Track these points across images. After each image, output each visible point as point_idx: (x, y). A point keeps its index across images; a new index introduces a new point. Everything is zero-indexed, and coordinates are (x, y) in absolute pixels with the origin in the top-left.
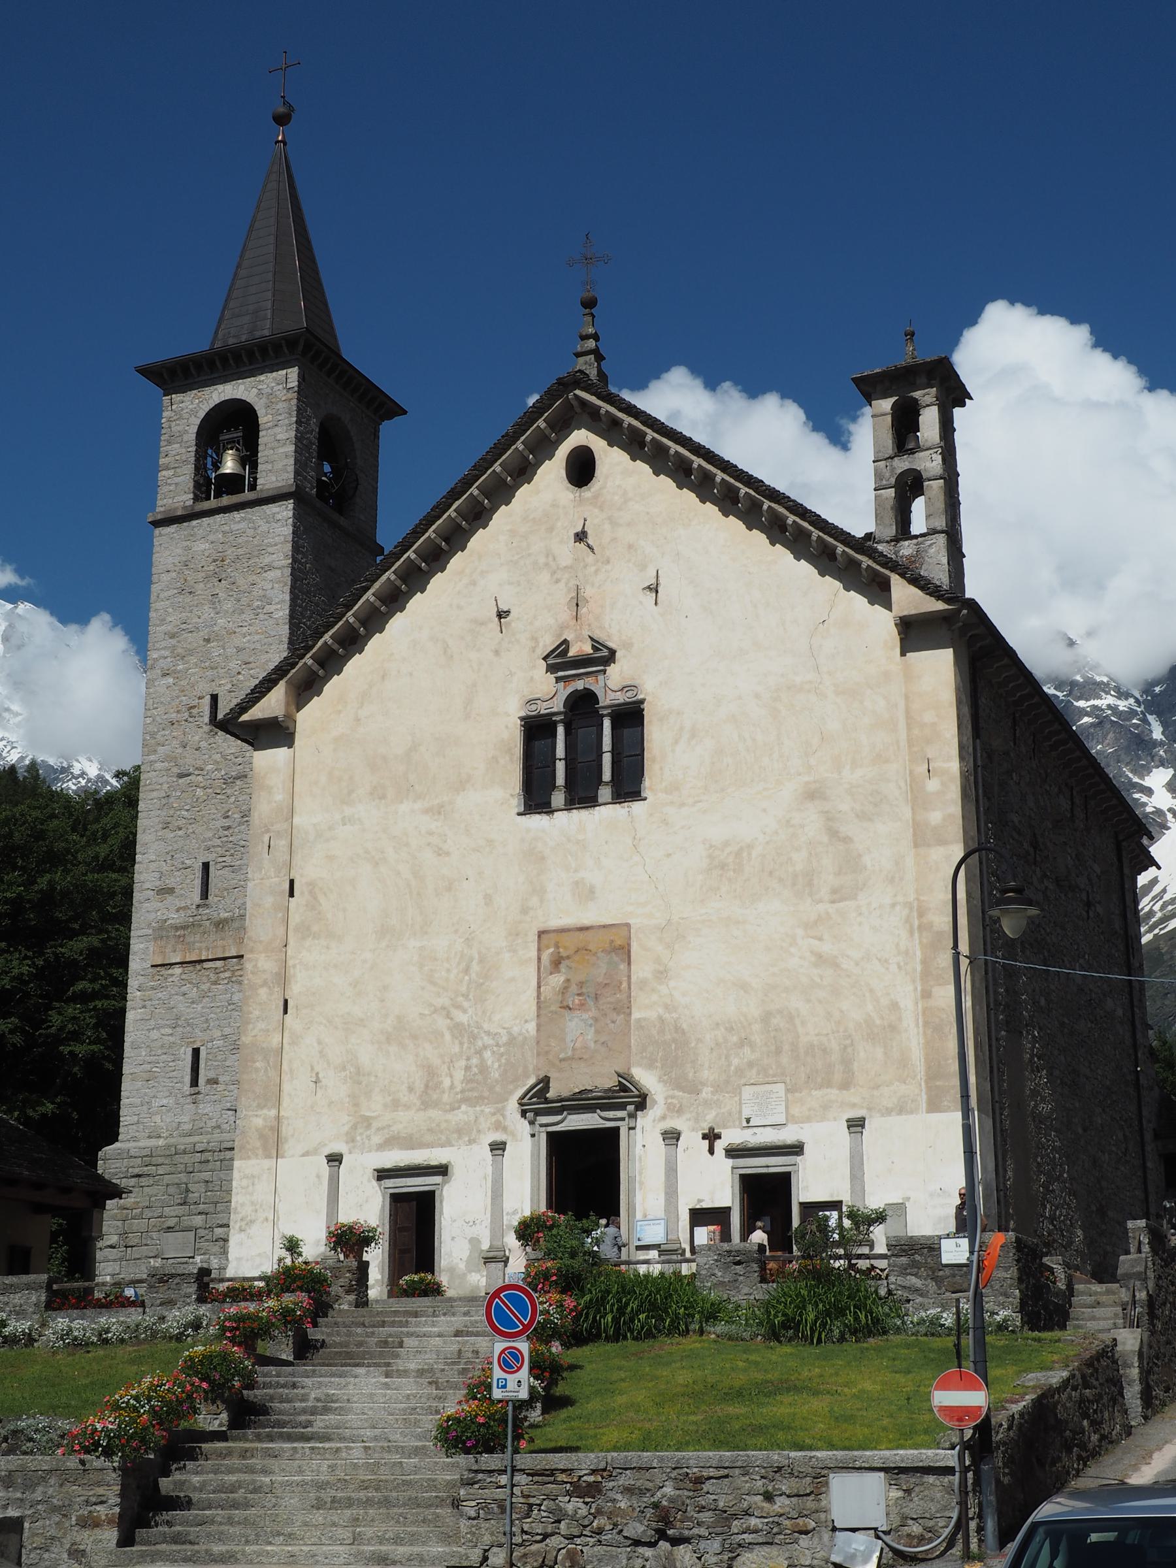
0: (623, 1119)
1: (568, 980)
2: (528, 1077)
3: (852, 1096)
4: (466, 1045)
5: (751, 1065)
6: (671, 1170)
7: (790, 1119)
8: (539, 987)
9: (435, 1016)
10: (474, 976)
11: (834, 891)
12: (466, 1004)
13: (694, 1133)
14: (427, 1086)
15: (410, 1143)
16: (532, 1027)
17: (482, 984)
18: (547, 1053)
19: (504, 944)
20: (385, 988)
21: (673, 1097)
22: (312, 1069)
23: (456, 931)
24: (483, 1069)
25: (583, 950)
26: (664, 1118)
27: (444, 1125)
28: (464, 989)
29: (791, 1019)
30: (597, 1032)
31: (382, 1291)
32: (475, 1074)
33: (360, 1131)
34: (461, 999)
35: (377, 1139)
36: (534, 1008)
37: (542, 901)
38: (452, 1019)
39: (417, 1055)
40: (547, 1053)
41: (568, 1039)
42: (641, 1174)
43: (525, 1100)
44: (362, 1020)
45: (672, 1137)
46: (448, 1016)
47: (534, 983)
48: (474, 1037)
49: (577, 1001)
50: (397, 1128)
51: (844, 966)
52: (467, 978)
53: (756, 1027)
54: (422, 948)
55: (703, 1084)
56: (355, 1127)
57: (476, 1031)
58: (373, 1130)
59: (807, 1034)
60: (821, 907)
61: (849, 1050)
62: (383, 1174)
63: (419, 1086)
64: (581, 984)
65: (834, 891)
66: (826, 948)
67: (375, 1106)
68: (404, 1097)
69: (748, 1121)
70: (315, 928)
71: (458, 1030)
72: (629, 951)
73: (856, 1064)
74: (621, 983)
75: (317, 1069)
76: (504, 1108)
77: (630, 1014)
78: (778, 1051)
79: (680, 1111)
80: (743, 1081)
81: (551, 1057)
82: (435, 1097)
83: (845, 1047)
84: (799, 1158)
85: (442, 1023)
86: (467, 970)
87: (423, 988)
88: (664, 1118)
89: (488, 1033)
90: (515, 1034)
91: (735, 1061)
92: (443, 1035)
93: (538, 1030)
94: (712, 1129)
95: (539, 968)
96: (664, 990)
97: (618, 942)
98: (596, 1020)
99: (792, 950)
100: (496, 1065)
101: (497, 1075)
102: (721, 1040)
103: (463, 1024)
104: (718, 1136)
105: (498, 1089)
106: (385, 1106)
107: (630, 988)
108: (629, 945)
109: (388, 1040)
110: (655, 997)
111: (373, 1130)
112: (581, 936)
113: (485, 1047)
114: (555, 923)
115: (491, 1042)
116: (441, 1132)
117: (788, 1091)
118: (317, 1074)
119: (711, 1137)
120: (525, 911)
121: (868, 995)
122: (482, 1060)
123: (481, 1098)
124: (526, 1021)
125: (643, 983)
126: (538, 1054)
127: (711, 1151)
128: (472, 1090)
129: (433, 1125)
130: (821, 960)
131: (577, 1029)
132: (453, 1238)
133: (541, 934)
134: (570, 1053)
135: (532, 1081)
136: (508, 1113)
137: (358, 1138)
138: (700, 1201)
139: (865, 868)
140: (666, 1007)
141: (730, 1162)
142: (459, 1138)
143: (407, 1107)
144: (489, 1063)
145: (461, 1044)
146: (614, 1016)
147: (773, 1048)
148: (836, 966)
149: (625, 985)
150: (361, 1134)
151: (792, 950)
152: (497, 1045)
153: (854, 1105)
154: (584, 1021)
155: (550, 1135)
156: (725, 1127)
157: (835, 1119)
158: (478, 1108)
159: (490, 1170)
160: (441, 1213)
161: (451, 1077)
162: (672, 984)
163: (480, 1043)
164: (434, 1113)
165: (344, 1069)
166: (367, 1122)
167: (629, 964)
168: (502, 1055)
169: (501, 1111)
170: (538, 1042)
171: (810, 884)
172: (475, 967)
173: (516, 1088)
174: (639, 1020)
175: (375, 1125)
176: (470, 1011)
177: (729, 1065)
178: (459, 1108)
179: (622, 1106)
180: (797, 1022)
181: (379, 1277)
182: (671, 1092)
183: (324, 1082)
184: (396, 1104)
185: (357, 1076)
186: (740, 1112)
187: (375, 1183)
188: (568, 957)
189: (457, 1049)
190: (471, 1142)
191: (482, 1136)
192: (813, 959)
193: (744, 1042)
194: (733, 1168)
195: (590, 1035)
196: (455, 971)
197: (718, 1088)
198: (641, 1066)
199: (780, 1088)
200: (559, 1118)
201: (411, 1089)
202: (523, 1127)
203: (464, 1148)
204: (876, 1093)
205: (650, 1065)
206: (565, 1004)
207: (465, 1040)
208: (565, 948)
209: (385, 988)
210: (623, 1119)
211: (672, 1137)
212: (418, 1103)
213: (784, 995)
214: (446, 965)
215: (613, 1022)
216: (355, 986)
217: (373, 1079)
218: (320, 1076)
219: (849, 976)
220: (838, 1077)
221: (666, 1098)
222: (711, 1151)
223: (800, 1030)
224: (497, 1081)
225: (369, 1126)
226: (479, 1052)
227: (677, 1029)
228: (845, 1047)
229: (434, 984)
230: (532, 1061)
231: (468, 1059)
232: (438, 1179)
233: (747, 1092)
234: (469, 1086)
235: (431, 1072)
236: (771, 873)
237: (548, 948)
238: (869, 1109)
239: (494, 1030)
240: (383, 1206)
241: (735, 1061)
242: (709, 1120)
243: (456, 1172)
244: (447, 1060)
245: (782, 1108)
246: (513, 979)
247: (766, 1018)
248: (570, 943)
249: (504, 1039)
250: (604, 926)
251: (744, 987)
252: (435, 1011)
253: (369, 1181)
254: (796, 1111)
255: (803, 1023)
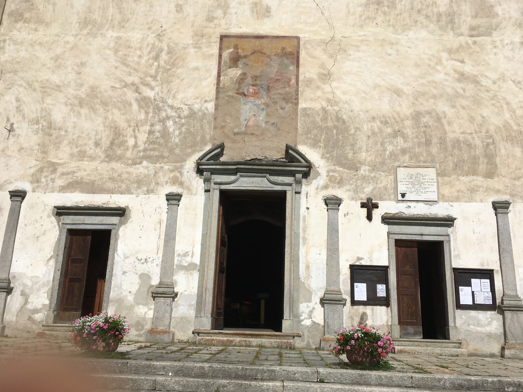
0: (290, 185)
1: (244, 74)
2: (205, 144)
3: (495, 183)
4: (151, 115)
5: (404, 151)
6: (333, 230)
7: (442, 198)
8: (219, 76)
9: (125, 90)
10: (162, 63)
11: (472, 28)
12: (153, 83)
13: (353, 202)
14: (112, 143)
15: (92, 188)
16: (211, 106)
17: (169, 70)
18: (223, 127)
19: (191, 42)
20: (83, 64)
21: (334, 171)
22: (8, 120)
23: (149, 28)
24: (165, 134)
25: (258, 52)
26: (326, 187)
27: (125, 176)
28: (153, 72)
29: (438, 119)
30: (268, 115)
31: (48, 316)
32: (157, 138)
33: (45, 174)
34: (149, 79)
35: (60, 182)
36: (214, 92)
37: (225, 14)
38: (140, 93)
39: (106, 118)
40: (223, 127)
41: (242, 118)
42: (304, 231)
43: (204, 161)
44: (59, 86)
45: (333, 203)
46: (137, 90)
47: (215, 73)
48: (158, 109)
49: (251, 90)
50: (79, 174)
51: (484, 84)
52: (156, 64)
53: (408, 123)
54: (119, 38)
55: (361, 163)
56: (41, 170)
57: (161, 105)
58: (58, 174)
59: (454, 132)
60: (461, 38)
61: (492, 147)
62: (61, 212)
63: (105, 142)
64: (255, 78)
65: (472, 29)
66: (468, 68)
67: (62, 155)
68: (91, 150)
69: (403, 195)
70: (27, 15)
71: (144, 102)
72: (298, 58)
73: (498, 160)
74: (290, 80)
75: (12, 120)
76: (182, 167)
77: (297, 104)
78: (428, 143)
79: (341, 183)
80: (397, 164)
81: (226, 131)
82: (119, 152)
83: (488, 145)
84: (450, 230)
85: (131, 95)
86: (157, 58)
87: (116, 68)
88: (326, 187)
89: (172, 107)
90: (196, 110)
91: (390, 148)
92: (130, 105)
93: (216, 109)
94: (369, 200)
95: (220, 63)
96: (327, 88)
97: (289, 50)
98: (267, 106)
99: (438, 68)
100: (177, 132)
101: (177, 140)
102: (376, 130)
103: (149, 98)
104: (376, 206)
105: (177, 151)
106: (72, 155)
107: (297, 84)
108: (298, 53)
109: (81, 105)
110: (319, 93)
111: (58, 174)
112: (257, 42)
113: (168, 118)
114: (235, 30)
115: (174, 114)
116: (122, 181)
117: (438, 174)
118: (12, 125)
119: (369, 206)
120: (210, 19)
121: (505, 106)
122: (165, 128)
123: (162, 157)
124: (206, 101)
125: (309, 82)
126: (215, 128)
127: (369, 217)
128: (154, 150)
129: (115, 175)
130: (462, 77)
131: (250, 112)
132: (124, 273)
133: (222, 37)
134: (243, 129)
135: (208, 148)
136: (185, 171)
137: (43, 180)
138: (359, 259)
139: (497, 15)
140: (329, 101)
141: (386, 228)
142: (139, 188)
143: (92, 158)
144: (171, 130)
145: (147, 113)
146: (284, 104)
147: (424, 140)
148: (476, 82)
149: (293, 81)
150: (46, 177)
151: (438, 68)
152: (179, 117)
153: (498, 191)
154: (257, 106)
155: (223, 194)
156: (381, 199)
157: (481, 201)
158: (158, 165)
159: (164, 217)
160: (115, 250)
161: (136, 137)
162: (334, 84)
163: (164, 114)
164: (116, 165)
165: (37, 122)
166: (54, 167)
167: (298, 66)
168: (183, 125)
169: (179, 169)
170: (215, 118)
171: (452, 22)
172: (164, 56)
173: (194, 152)
174: (305, 109)
175: (60, 170)
176: (157, 89)
177: (385, 150)
178: (141, 163)
179: (292, 174)
180: (444, 121)
181: (47, 302)
182: (333, 167)
183: (18, 131)
184: (82, 155)
185: (49, 130)
186: (396, 188)
187: (53, 219)
188: (245, 57)
189: (143, 116)
190: (149, 192)
191: (160, 188)
192: (456, 76)
193: (396, 134)
194: (389, 233)
195: (262, 117)
196: (146, 58)
197: (374, 168)
198: (306, 144)
199: (431, 173)
200: (233, 178)
201: (97, 144)
202: (198, 183)
203: (141, 196)
204: (517, 183)
205: (314, 145)
206: (241, 91)
207: (151, 110)
208: (243, 49)
209: (83, 64)
210: (290, 185)
211: (333, 203)
212: (103, 156)
213: (432, 101)
214: (138, 52)
215: (283, 109)
216: (56, 60)
217: (63, 133)
218: (15, 126)
219: (488, 91)
220: (483, 167)
221: (328, 172)
222: (369, 217)
223: (447, 128)
224: (177, 145)
225: (54, 171)
226: (163, 121)
227: (338, 119)
228: (488, 145)
229: (127, 66)
230: (209, 132)
231: (152, 125)
232: (115, 220)
233: (402, 173)
234: (151, 146)
235: (117, 134)
236: (419, 11)
237: (228, 48)
238: (513, 196)
239: (177, 104)
240: (59, 240)
241: (390, 148)
242: (367, 191)
243: (134, 215)
244: (133, 124)
245: (435, 188)
246: (196, 69)
247: (417, 116)
248: (247, 47)
249: (186, 113)
250: (277, 37)
251: (398, 92)
252: (126, 86)
253: (49, 217)
254: (446, 191)
255: (450, 123)
